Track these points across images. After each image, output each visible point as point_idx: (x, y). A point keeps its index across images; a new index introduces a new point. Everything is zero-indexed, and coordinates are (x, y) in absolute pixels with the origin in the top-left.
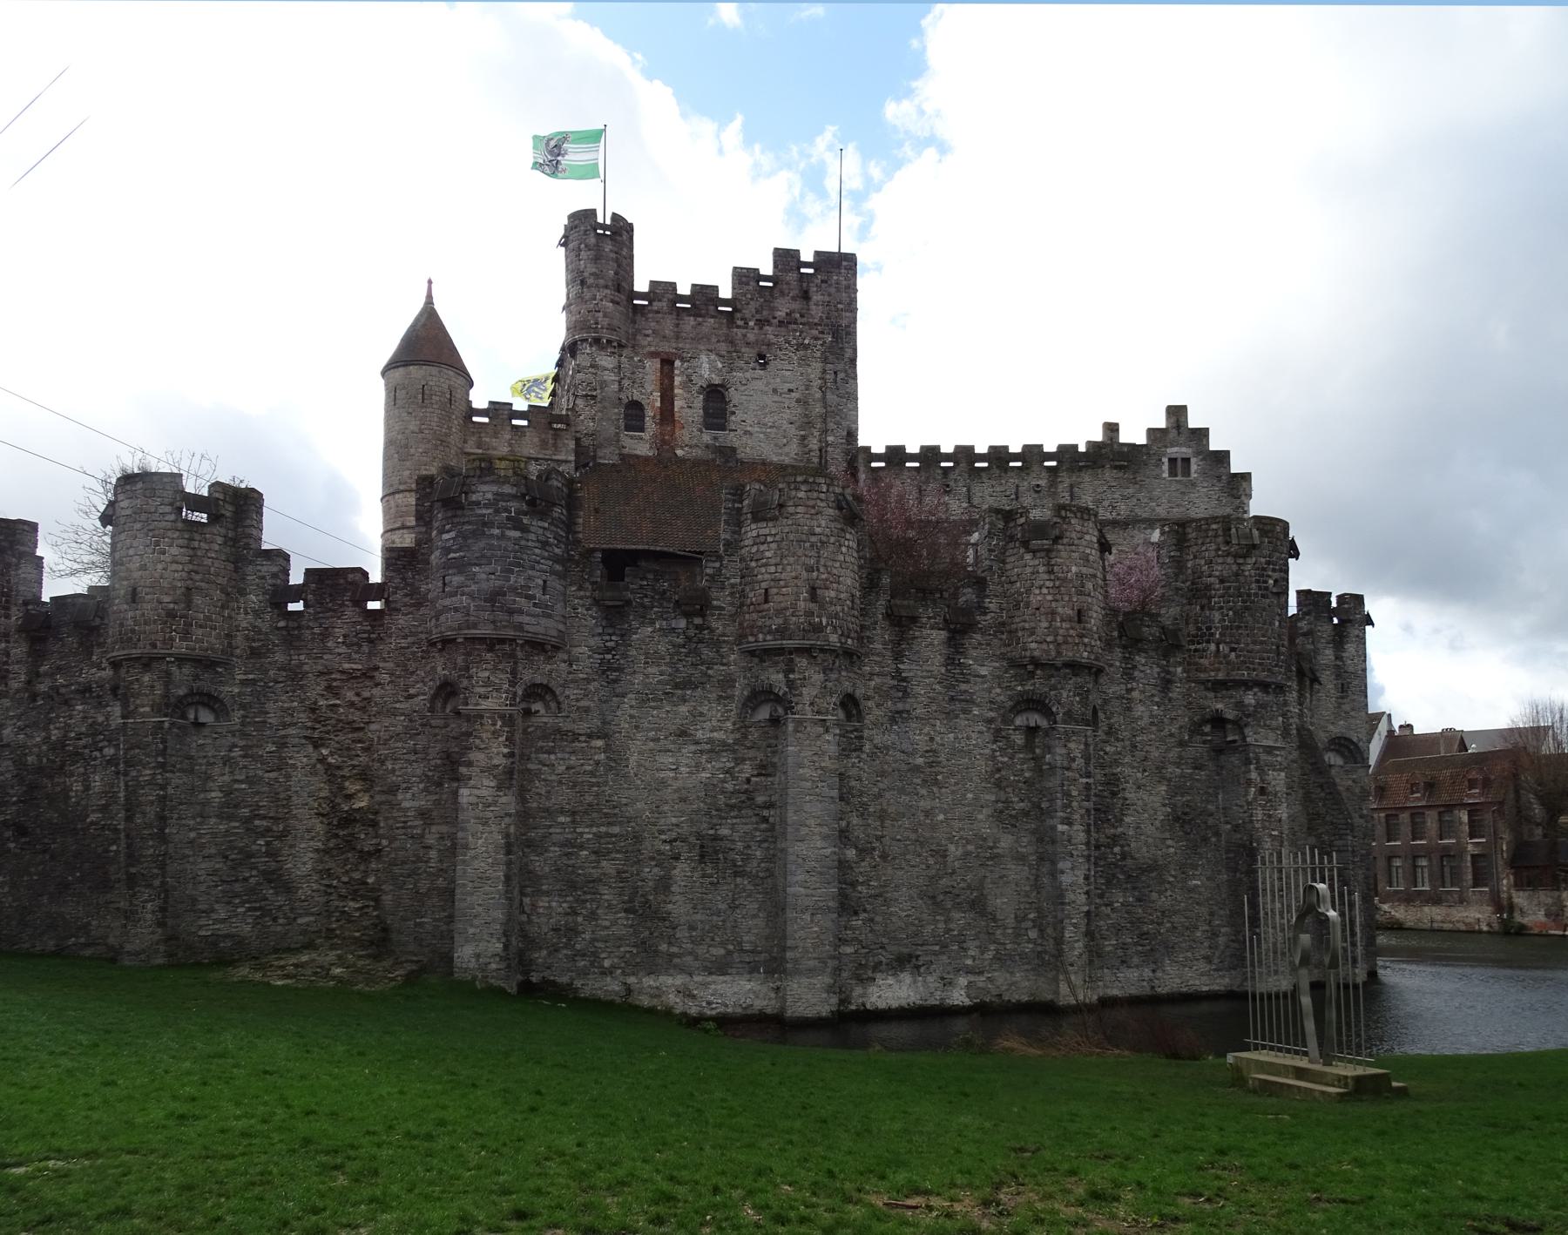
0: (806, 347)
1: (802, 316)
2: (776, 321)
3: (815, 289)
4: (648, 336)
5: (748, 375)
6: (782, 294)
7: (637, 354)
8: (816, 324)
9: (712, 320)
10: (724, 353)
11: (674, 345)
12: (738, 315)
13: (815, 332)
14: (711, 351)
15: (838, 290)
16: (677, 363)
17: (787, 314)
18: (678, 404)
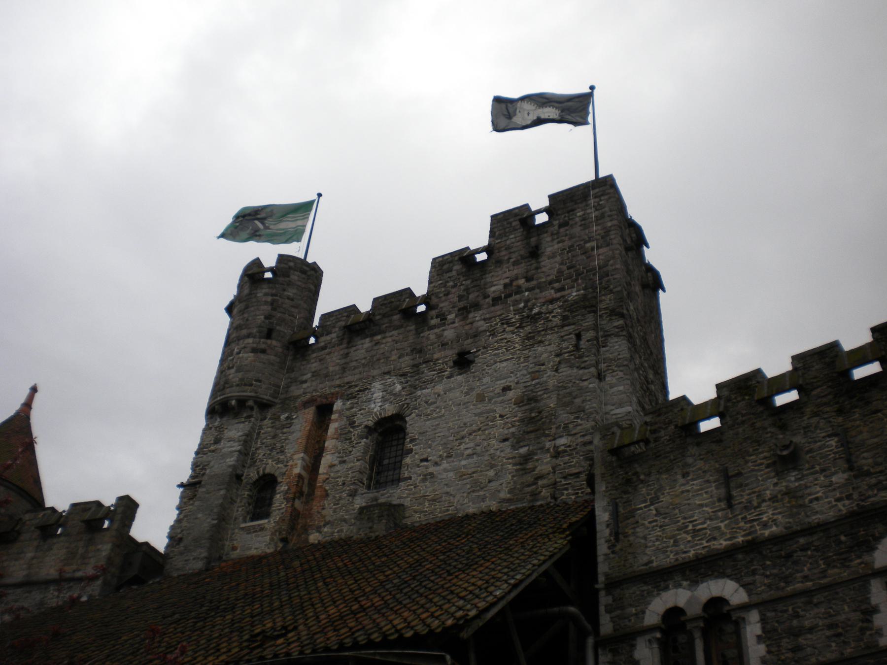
0: (534, 319)
1: (528, 279)
2: (489, 300)
3: (549, 239)
4: (305, 382)
5: (439, 388)
6: (499, 263)
7: (284, 410)
8: (551, 283)
9: (395, 333)
10: (408, 369)
11: (338, 382)
12: (433, 313)
13: (551, 293)
14: (388, 373)
15: (585, 227)
16: (338, 405)
17: (505, 286)
18: (327, 459)
